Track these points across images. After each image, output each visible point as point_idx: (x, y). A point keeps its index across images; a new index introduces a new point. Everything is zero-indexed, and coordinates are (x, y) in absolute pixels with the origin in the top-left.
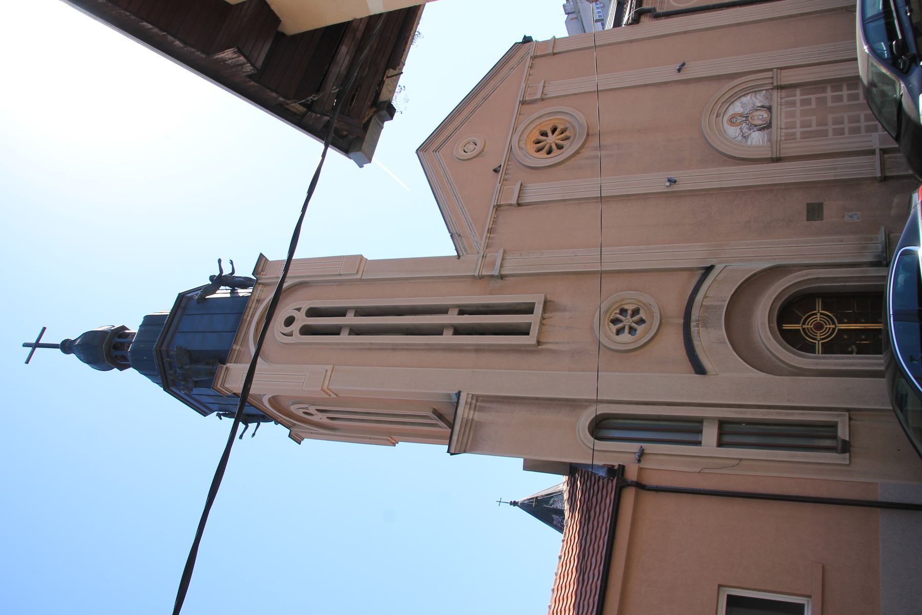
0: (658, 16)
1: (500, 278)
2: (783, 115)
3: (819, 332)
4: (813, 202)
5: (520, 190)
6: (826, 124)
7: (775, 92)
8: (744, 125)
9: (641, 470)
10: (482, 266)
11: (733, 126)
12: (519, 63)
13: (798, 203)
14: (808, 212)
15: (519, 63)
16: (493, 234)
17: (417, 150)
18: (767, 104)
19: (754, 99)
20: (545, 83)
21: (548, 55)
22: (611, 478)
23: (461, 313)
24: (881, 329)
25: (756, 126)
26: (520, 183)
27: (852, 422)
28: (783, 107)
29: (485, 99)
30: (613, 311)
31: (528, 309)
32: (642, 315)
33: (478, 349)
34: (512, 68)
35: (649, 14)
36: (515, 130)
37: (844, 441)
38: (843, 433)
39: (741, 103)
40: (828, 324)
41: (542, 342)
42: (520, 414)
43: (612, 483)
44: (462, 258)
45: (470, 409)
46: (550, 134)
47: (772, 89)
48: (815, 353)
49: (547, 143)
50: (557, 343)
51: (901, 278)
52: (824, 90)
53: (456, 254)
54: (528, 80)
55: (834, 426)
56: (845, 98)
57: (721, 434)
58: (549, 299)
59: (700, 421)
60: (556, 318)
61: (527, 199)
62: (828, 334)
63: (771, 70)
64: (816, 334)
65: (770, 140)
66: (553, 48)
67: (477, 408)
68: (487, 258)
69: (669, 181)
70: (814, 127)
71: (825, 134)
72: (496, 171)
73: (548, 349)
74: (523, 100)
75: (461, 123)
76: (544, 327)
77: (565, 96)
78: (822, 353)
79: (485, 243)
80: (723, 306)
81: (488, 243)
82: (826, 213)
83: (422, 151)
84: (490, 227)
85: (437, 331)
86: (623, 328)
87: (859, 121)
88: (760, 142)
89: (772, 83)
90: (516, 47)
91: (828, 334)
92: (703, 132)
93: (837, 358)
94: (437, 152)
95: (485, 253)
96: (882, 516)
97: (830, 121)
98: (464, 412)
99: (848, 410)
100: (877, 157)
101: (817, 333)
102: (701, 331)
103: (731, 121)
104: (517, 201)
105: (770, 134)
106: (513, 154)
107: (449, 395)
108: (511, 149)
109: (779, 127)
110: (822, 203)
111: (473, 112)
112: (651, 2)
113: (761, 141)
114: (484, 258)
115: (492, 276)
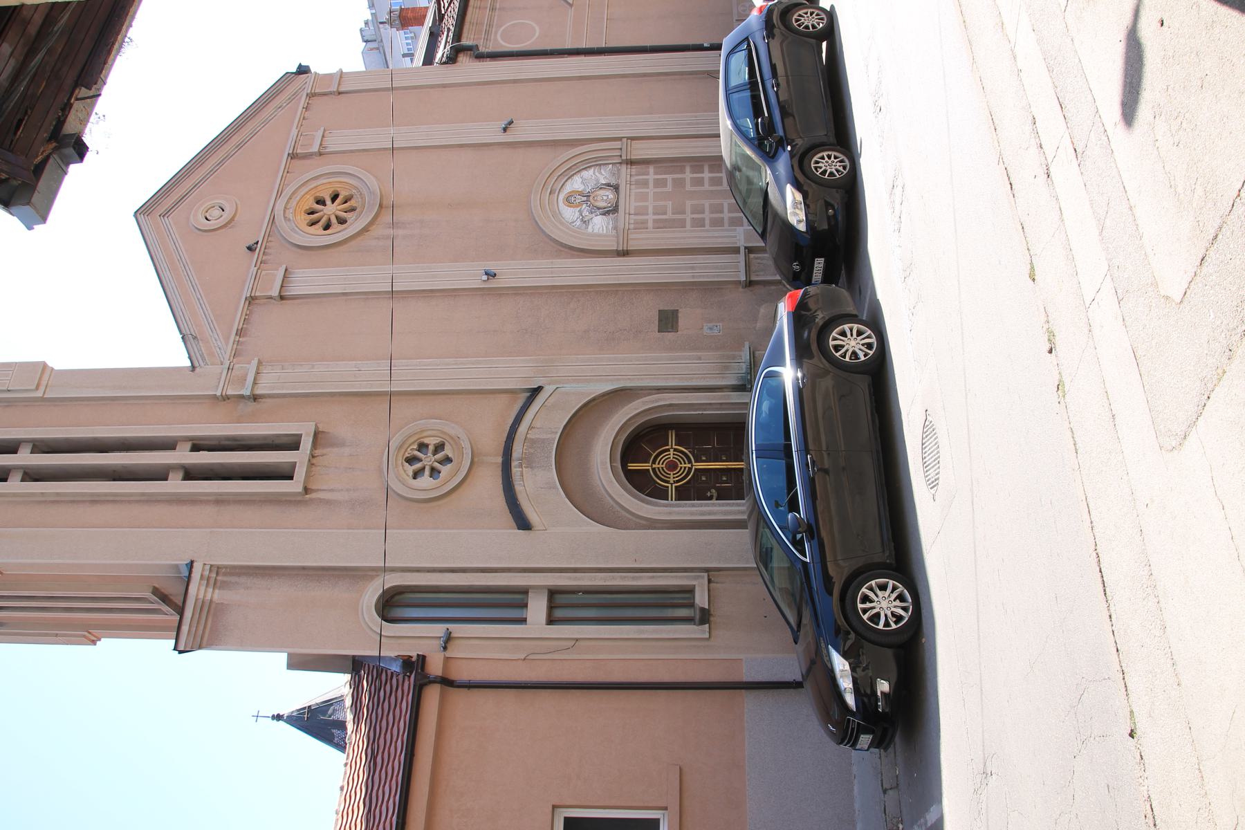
0: (481, 57)
1: (252, 400)
2: (633, 197)
3: (672, 473)
4: (666, 309)
5: (285, 277)
6: (684, 213)
7: (624, 167)
8: (584, 206)
9: (447, 659)
10: (227, 383)
11: (571, 207)
12: (290, 100)
13: (648, 309)
14: (660, 320)
15: (290, 100)
16: (243, 336)
17: (135, 213)
18: (613, 182)
19: (597, 174)
20: (325, 130)
21: (331, 93)
22: (408, 674)
23: (196, 448)
24: (742, 469)
25: (599, 208)
26: (284, 267)
27: (712, 585)
28: (633, 187)
29: (240, 146)
30: (408, 448)
31: (292, 444)
32: (448, 451)
33: (220, 500)
34: (280, 108)
35: (469, 52)
36: (279, 194)
37: (702, 609)
38: (701, 599)
39: (581, 178)
40: (683, 463)
41: (313, 490)
42: (280, 591)
43: (409, 680)
44: (198, 370)
45: (207, 585)
46: (329, 202)
47: (620, 163)
48: (668, 500)
49: (325, 214)
50: (332, 490)
51: (765, 406)
52: (682, 171)
53: (190, 364)
55: (690, 591)
56: (706, 182)
57: (551, 607)
58: (320, 430)
59: (524, 591)
60: (330, 455)
61: (294, 289)
62: (683, 476)
63: (620, 139)
64: (668, 476)
65: (615, 228)
66: (339, 84)
67: (218, 584)
68: (234, 370)
69: (487, 274)
70: (669, 216)
71: (682, 224)
72: (250, 248)
73: (320, 499)
74: (293, 153)
75: (201, 180)
76: (314, 468)
77: (352, 151)
78: (675, 500)
79: (232, 350)
80: (555, 438)
82: (682, 322)
83: (143, 213)
84: (240, 328)
85: (160, 474)
86: (423, 469)
87: (722, 212)
88: (603, 230)
89: (621, 156)
90: (287, 78)
91: (683, 476)
92: (532, 213)
93: (693, 506)
94: (166, 218)
95: (232, 364)
96: (749, 701)
97: (688, 209)
98: (198, 589)
99: (707, 570)
100: (741, 257)
101: (670, 474)
102: (524, 473)
103: (569, 201)
104: (280, 292)
105: (616, 221)
106: (276, 226)
107: (177, 566)
108: (273, 220)
109: (627, 211)
110: (678, 310)
111: (221, 163)
112: (472, 37)
113: (605, 228)
114: (230, 371)
115: (242, 397)
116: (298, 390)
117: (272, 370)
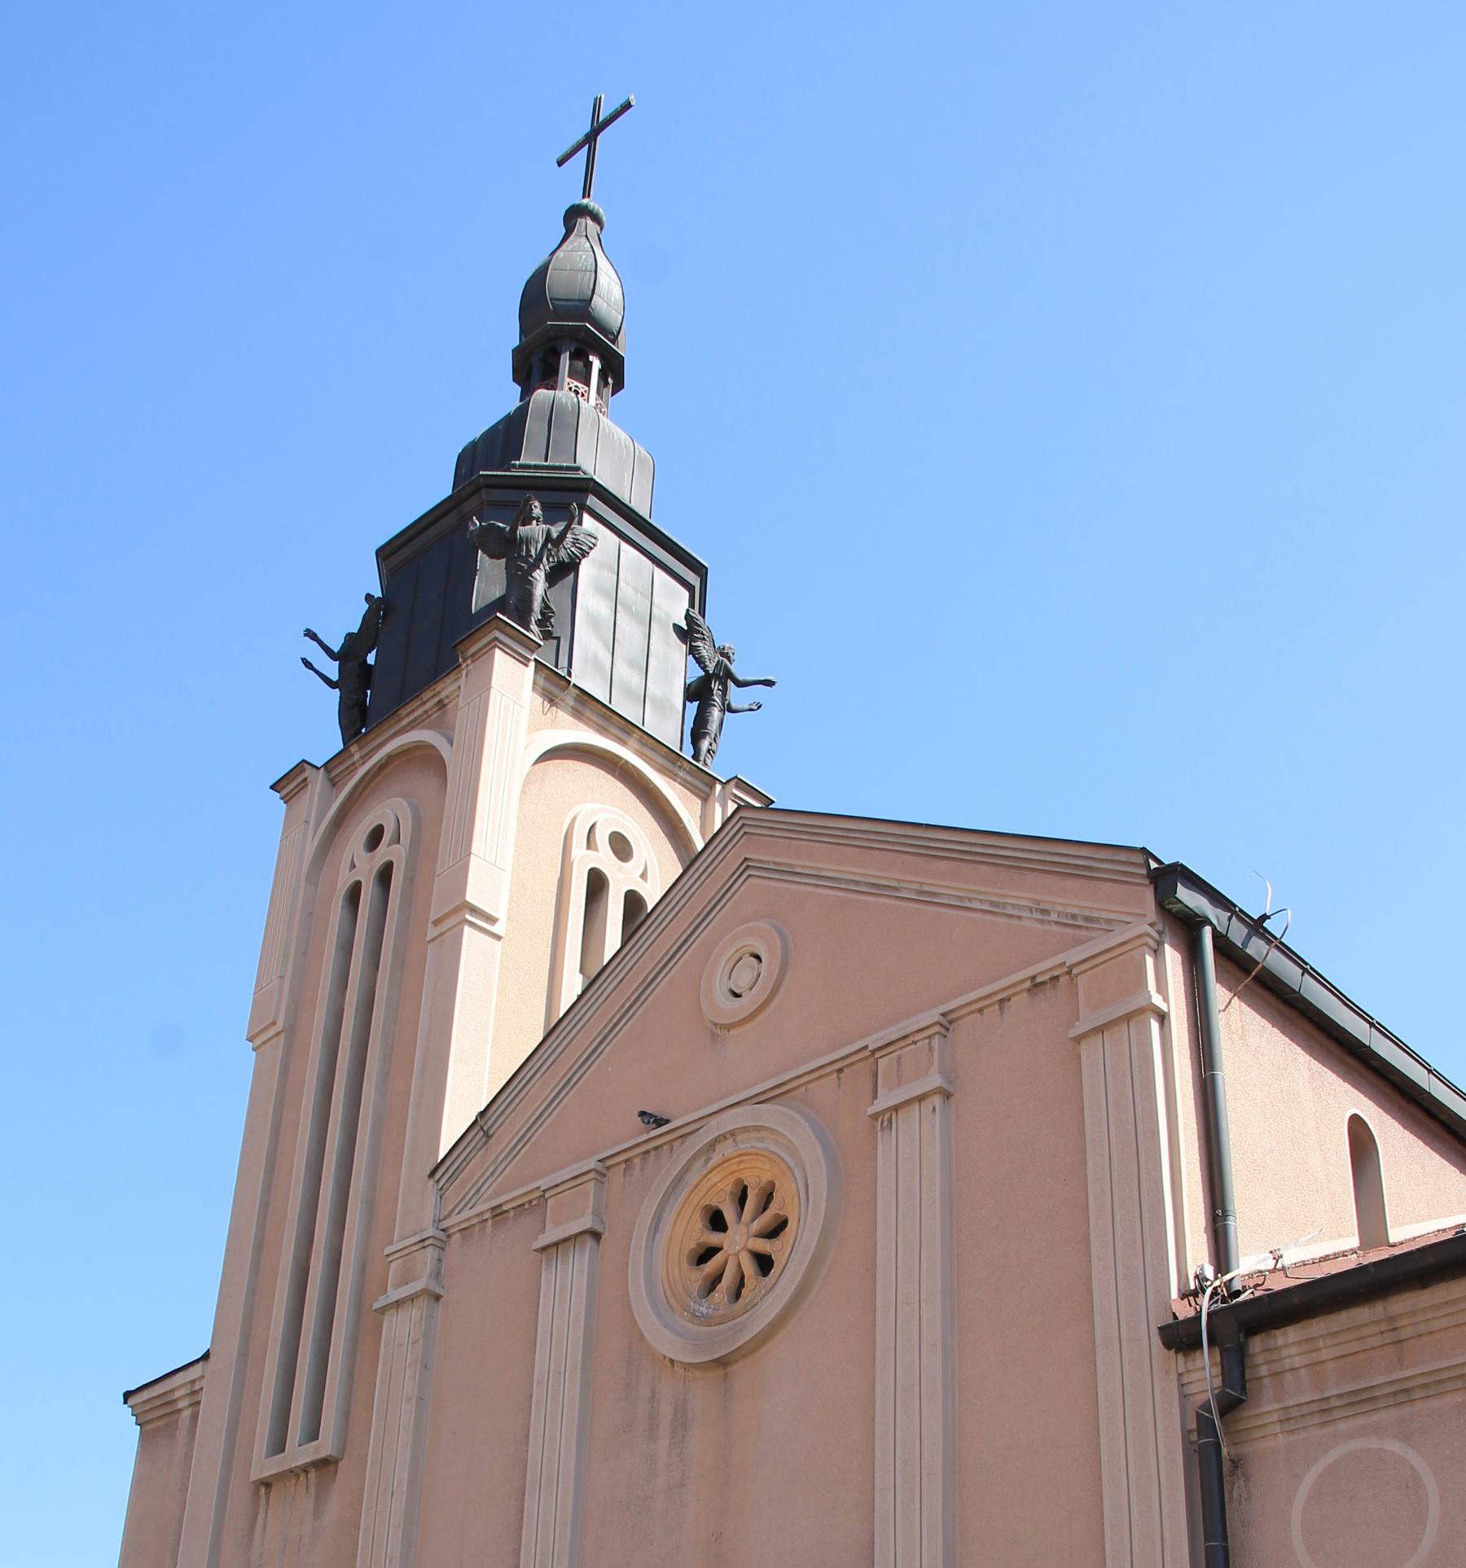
12: (1071, 922)
44: (431, 1182)
54: (980, 1011)
73: (257, 1514)
81: (472, 1225)
84: (505, 1208)
114: (420, 1245)
116: (378, 1393)
117: (415, 1325)
